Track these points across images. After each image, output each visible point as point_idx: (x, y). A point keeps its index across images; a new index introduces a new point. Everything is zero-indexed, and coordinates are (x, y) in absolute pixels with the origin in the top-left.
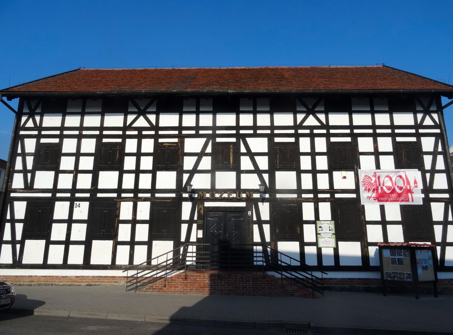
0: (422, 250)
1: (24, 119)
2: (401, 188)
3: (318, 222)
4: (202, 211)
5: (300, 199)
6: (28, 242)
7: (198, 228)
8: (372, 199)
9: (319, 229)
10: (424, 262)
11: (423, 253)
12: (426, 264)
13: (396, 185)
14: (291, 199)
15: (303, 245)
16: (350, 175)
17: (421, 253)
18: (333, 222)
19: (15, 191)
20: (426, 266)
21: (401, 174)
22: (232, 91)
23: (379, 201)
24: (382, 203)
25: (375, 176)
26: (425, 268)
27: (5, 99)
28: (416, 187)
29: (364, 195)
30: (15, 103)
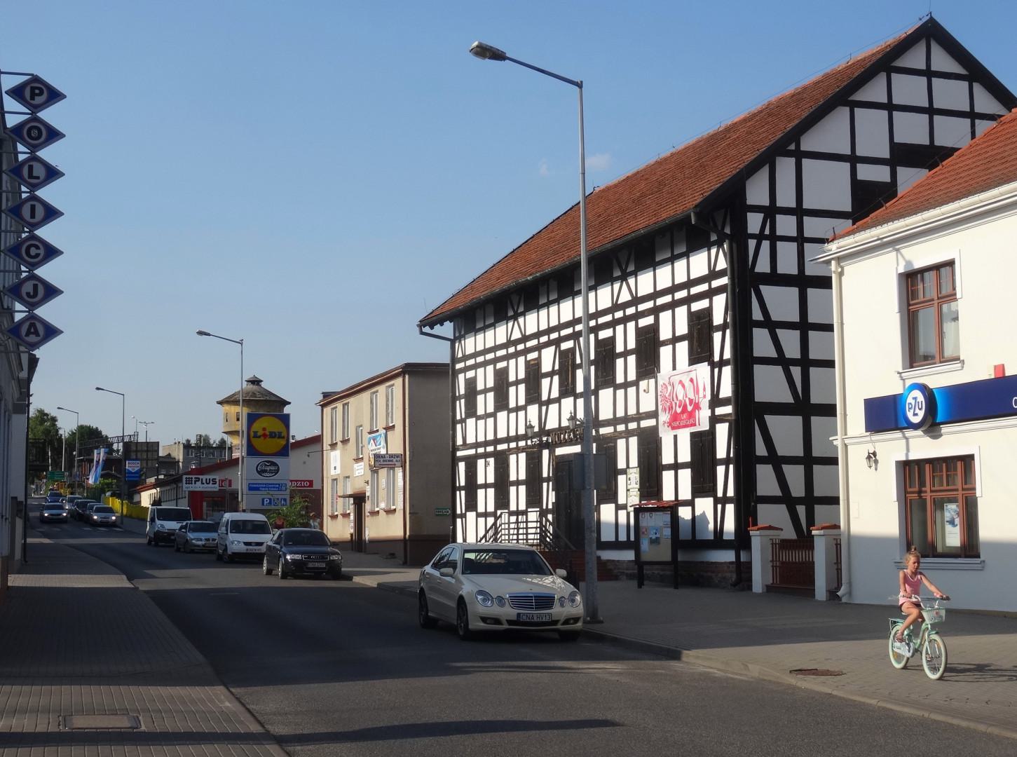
0: (654, 513)
1: (457, 345)
2: (691, 401)
3: (628, 470)
4: (554, 463)
5: (616, 434)
6: (468, 513)
7: (553, 490)
8: (666, 425)
9: (629, 482)
10: (655, 531)
11: (653, 517)
12: (658, 535)
13: (686, 397)
14: (609, 435)
15: (618, 507)
16: (652, 381)
17: (651, 517)
18: (638, 469)
19: (459, 450)
20: (657, 538)
21: (693, 375)
22: (531, 277)
23: (673, 428)
24: (675, 432)
25: (670, 383)
26: (655, 542)
27: (427, 329)
28: (705, 396)
29: (664, 417)
30: (447, 329)
